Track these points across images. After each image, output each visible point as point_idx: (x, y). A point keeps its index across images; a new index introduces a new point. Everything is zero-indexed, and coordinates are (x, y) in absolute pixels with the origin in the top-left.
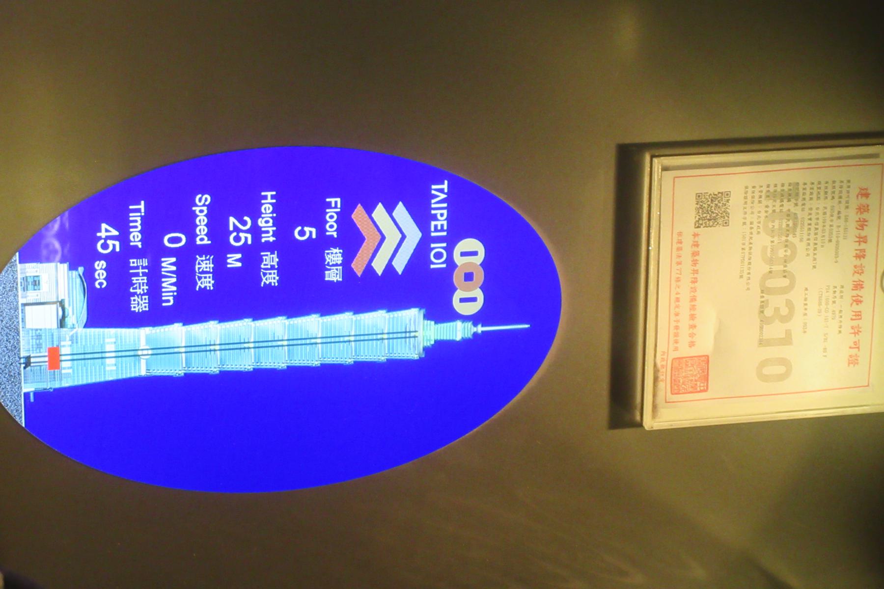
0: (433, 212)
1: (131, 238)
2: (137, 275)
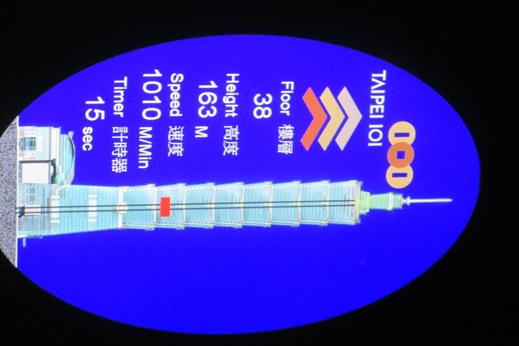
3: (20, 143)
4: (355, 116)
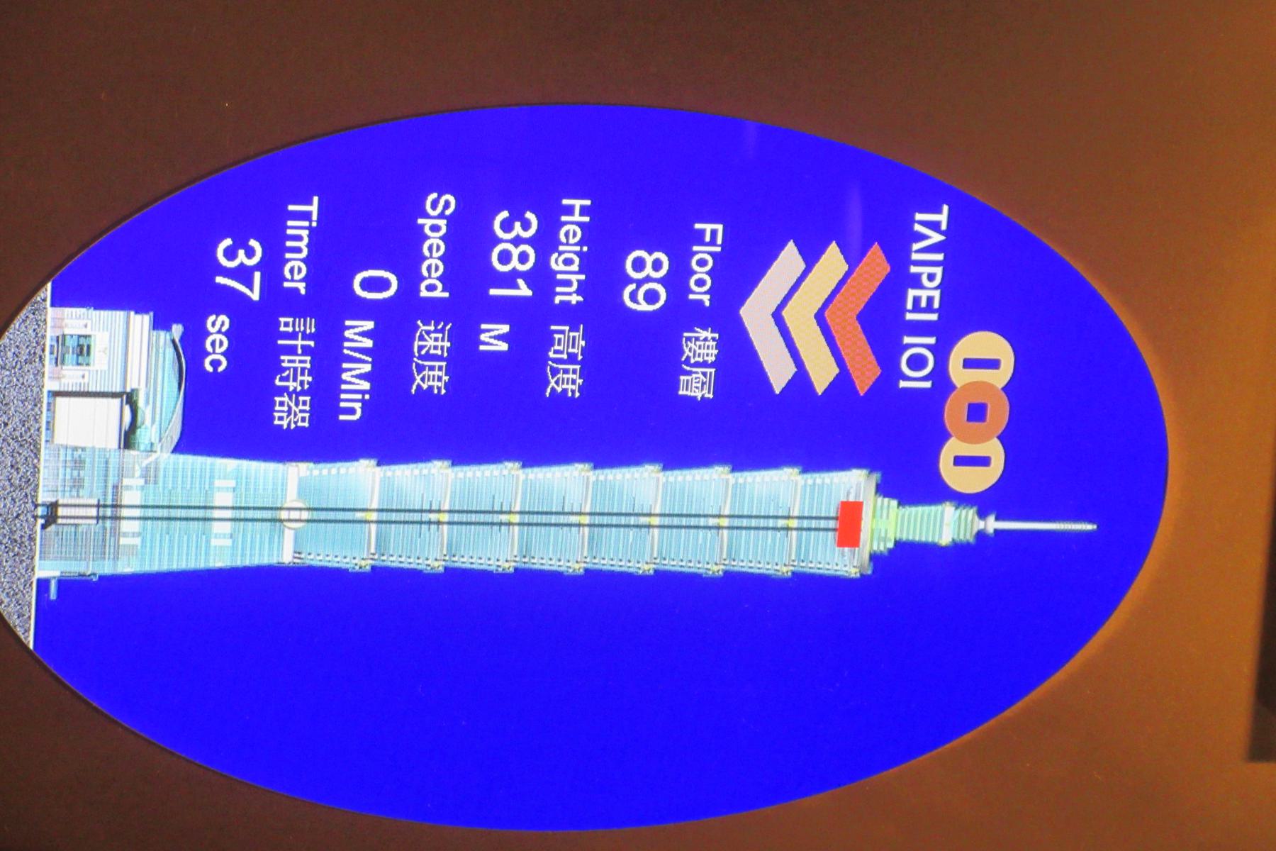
2: (291, 350)
3: (52, 346)
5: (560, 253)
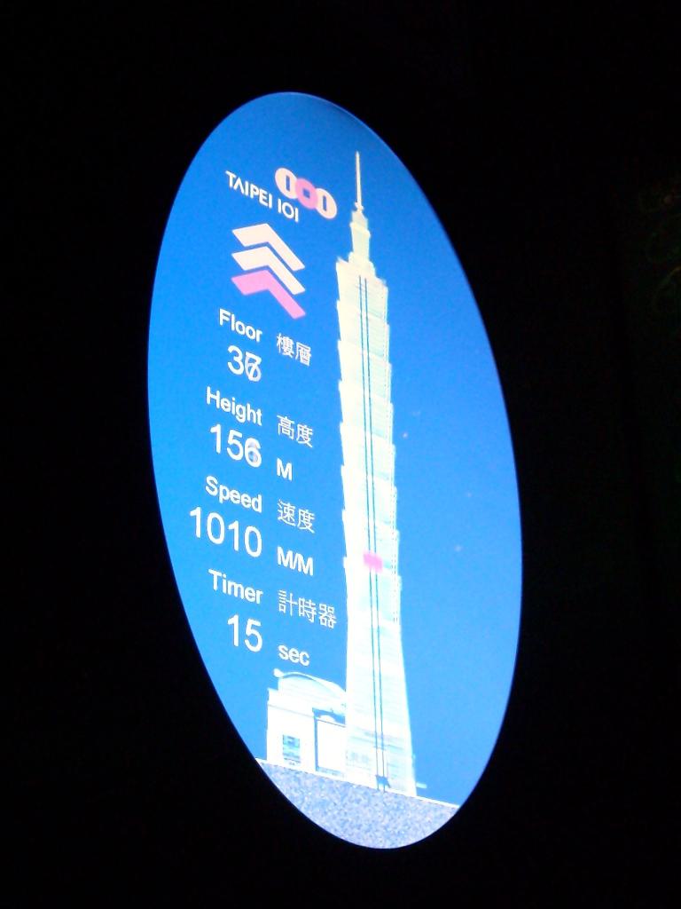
0: (252, 196)
1: (252, 600)
2: (296, 608)
3: (290, 764)
4: (264, 232)
5: (236, 414)
